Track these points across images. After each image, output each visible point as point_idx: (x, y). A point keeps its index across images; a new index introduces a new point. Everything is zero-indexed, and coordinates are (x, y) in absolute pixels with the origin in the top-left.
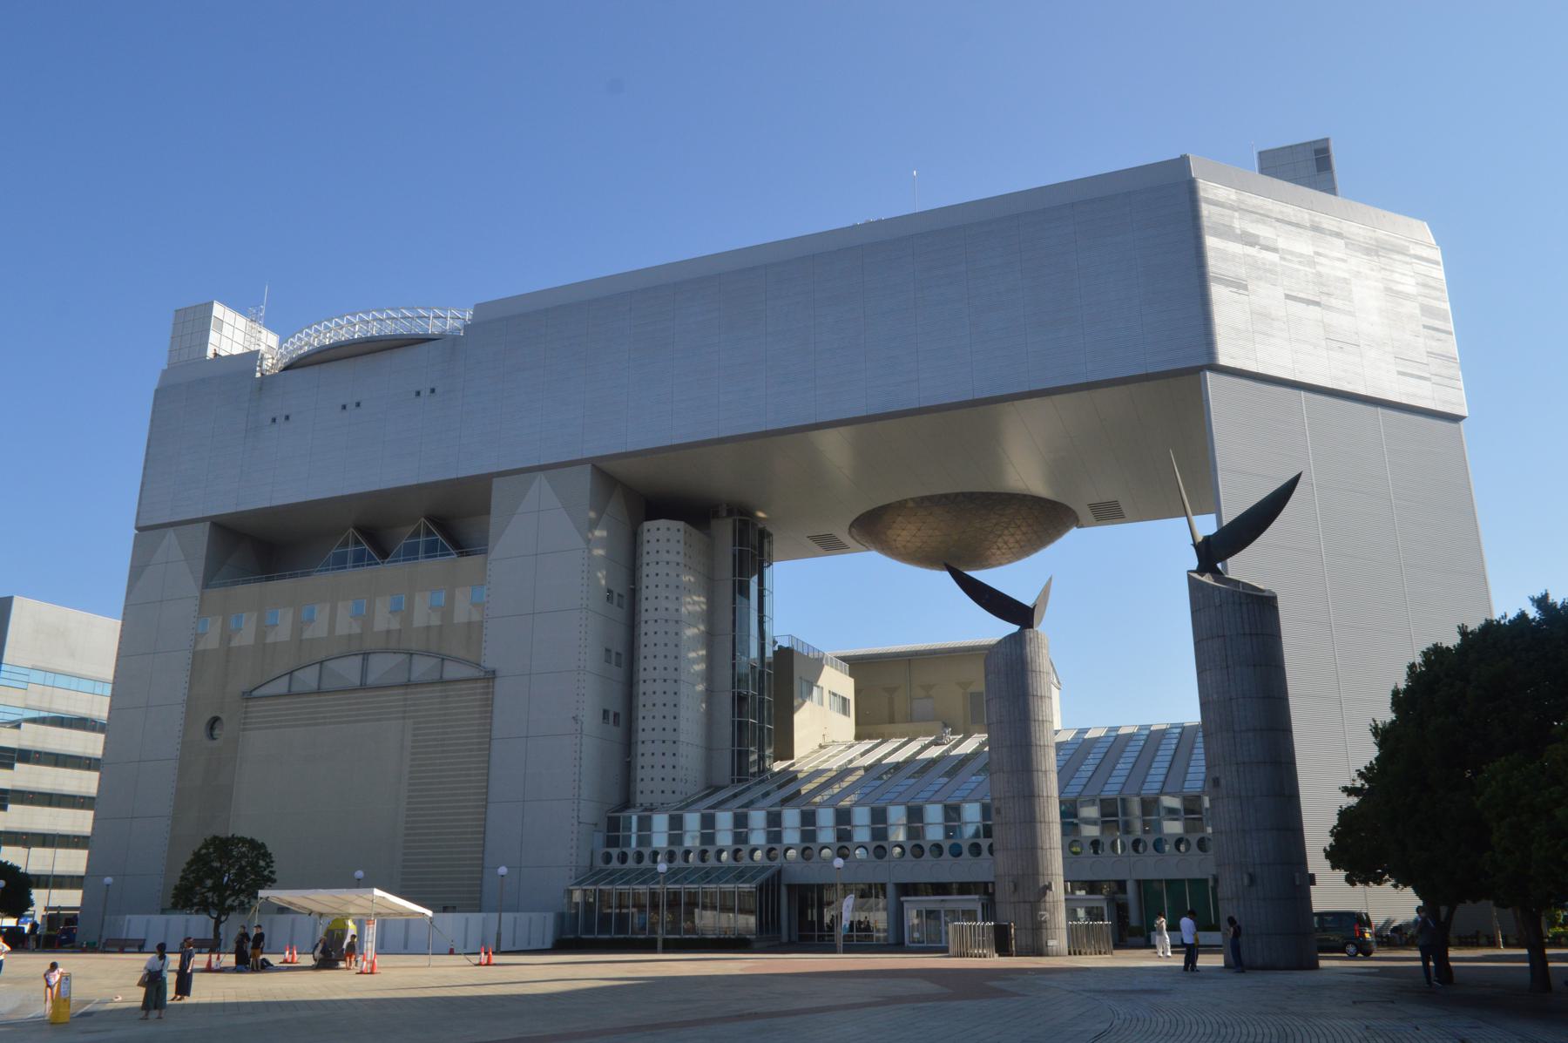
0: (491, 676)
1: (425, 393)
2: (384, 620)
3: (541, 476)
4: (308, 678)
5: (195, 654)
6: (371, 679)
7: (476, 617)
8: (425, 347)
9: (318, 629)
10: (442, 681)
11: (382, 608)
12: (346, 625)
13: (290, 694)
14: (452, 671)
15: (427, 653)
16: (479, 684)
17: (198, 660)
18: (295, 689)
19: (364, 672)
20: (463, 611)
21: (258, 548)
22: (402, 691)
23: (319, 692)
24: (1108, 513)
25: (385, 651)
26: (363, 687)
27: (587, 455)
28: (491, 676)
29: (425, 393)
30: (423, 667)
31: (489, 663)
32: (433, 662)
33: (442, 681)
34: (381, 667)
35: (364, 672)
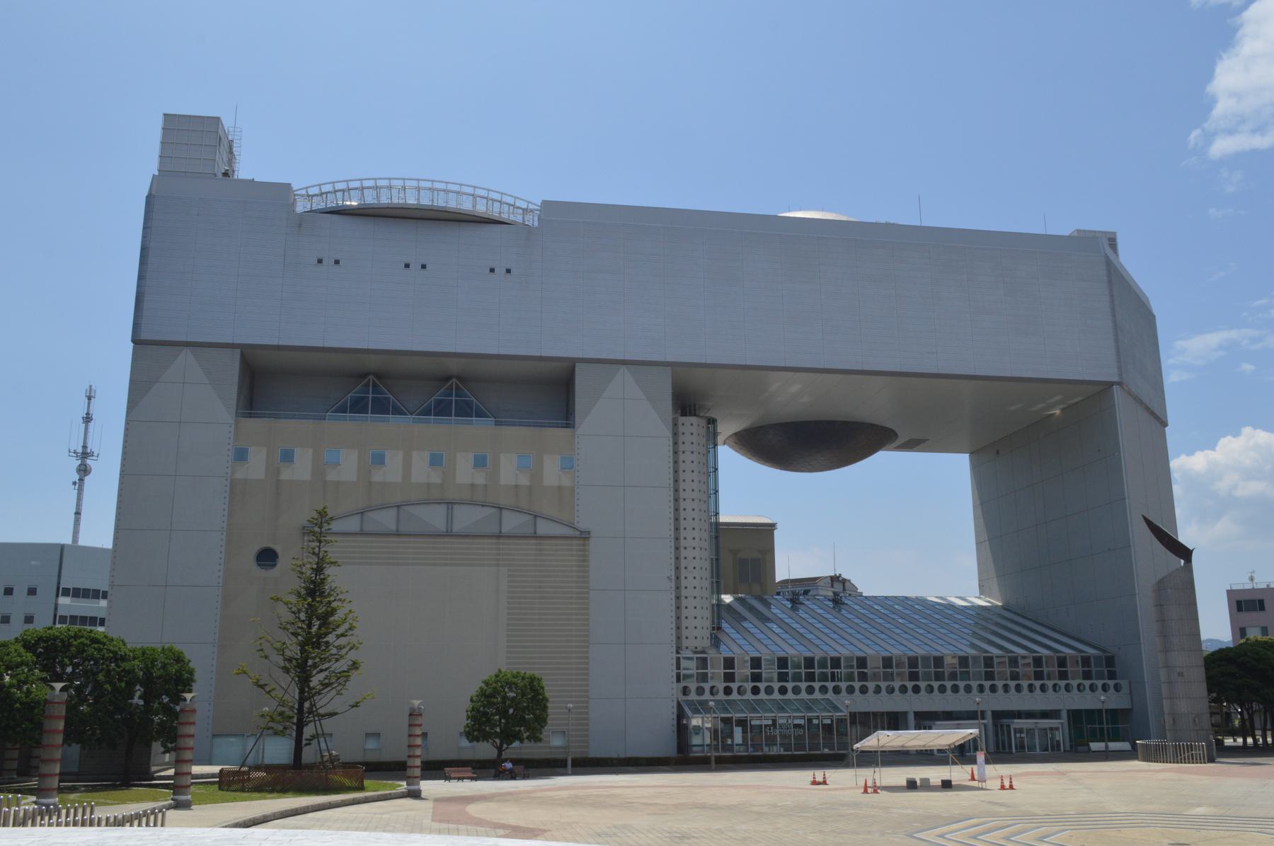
0: (585, 536)
1: (500, 271)
2: (465, 472)
3: (623, 370)
4: (387, 519)
5: (234, 483)
6: (457, 528)
7: (566, 482)
8: (499, 226)
9: (391, 472)
10: (535, 536)
11: (420, 461)
12: (422, 472)
13: (362, 533)
14: (544, 528)
15: (517, 510)
16: (575, 542)
17: (237, 492)
18: (368, 528)
19: (450, 520)
20: (552, 473)
21: (265, 381)
22: (494, 541)
23: (398, 534)
24: (912, 445)
25: (472, 503)
26: (449, 534)
27: (670, 359)
28: (585, 536)
29: (500, 271)
30: (511, 522)
31: (583, 525)
32: (524, 518)
33: (535, 536)
34: (466, 518)
35: (450, 520)
